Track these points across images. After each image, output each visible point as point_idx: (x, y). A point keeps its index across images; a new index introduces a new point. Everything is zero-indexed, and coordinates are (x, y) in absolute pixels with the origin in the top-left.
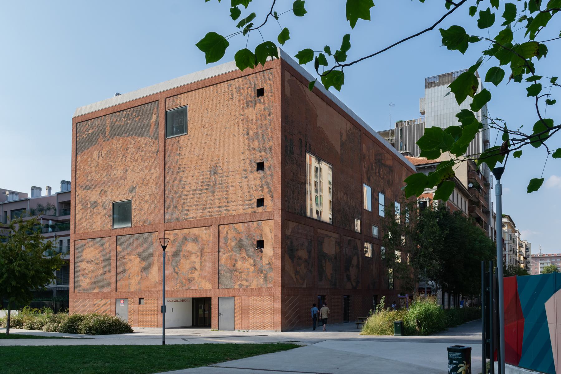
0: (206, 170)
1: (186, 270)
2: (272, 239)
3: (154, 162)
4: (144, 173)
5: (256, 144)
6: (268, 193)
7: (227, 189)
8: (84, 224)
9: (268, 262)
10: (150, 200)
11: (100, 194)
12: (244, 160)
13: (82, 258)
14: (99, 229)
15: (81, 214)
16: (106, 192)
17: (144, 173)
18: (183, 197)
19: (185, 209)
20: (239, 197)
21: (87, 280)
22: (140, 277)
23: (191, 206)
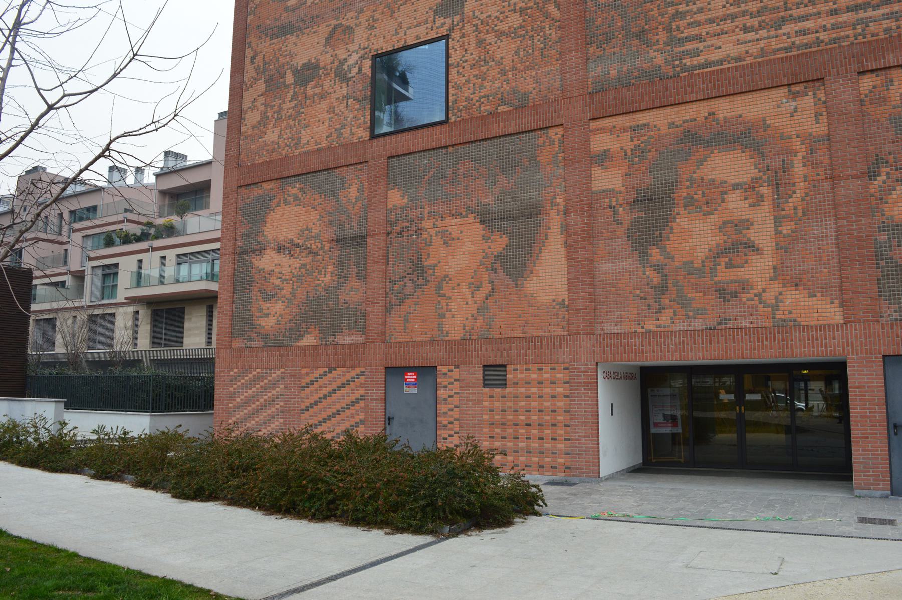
1: (701, 253)
8: (271, 136)
10: (521, 26)
11: (327, 39)
13: (260, 239)
14: (324, 144)
15: (262, 108)
16: (349, 30)
21: (278, 307)
22: (486, 288)
23: (711, 21)
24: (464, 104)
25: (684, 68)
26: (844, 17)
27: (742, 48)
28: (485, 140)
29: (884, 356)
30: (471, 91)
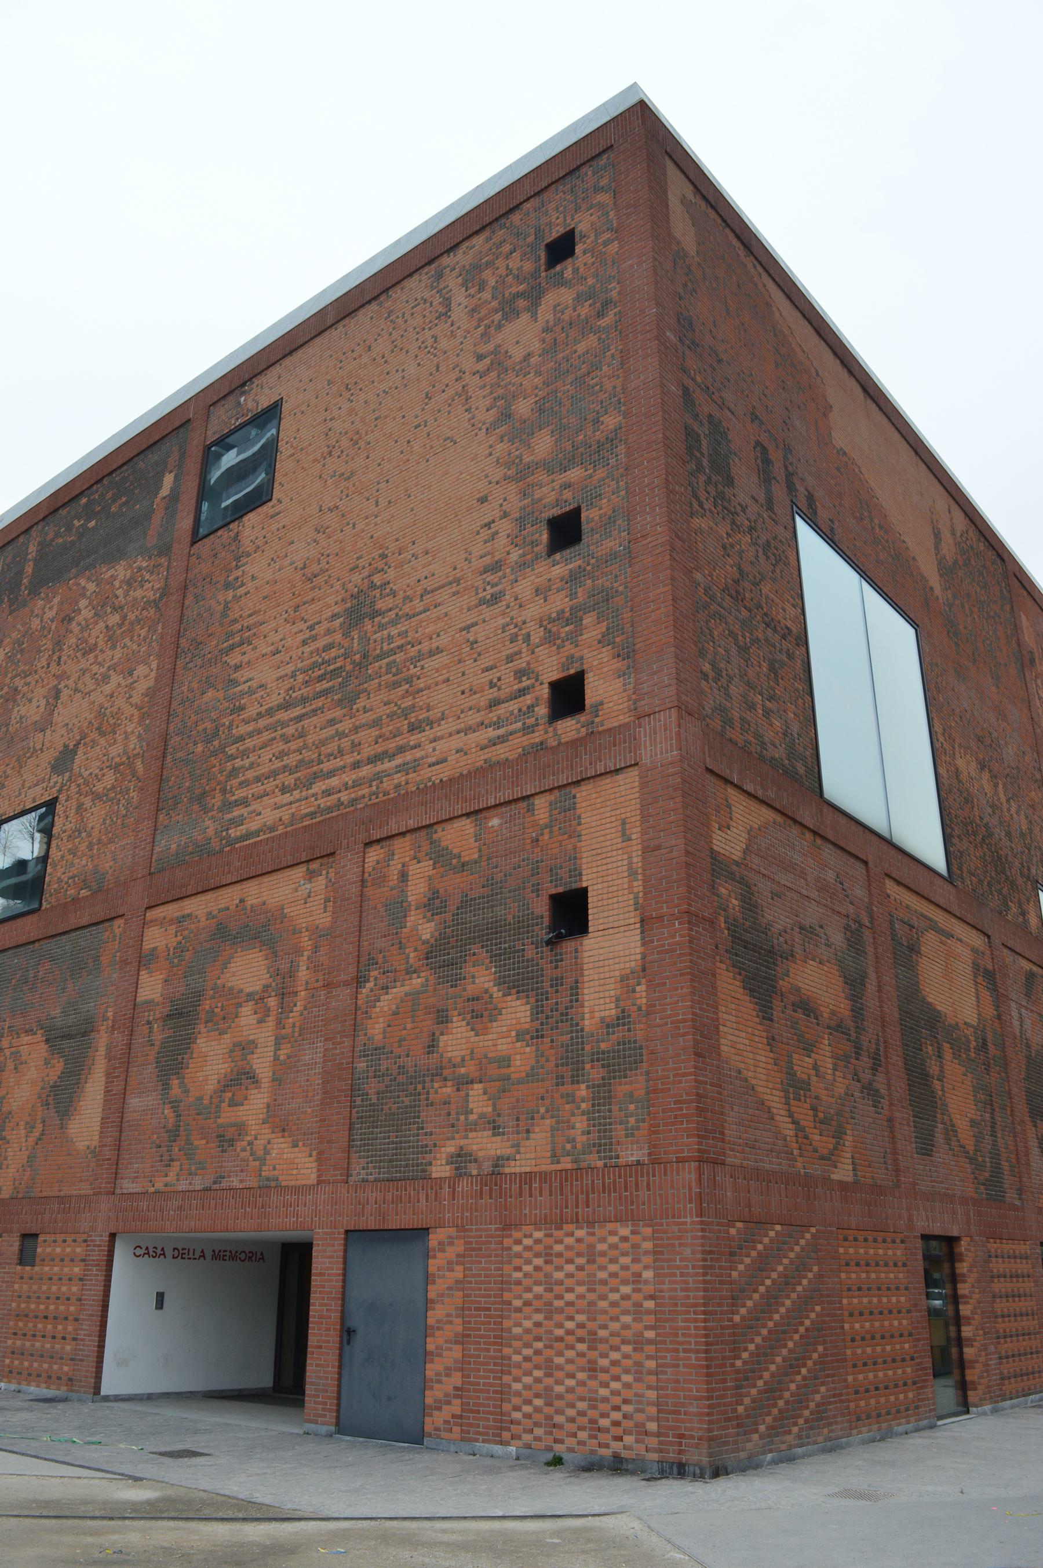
0: (330, 614)
1: (211, 1086)
2: (632, 873)
3: (145, 640)
4: (108, 689)
5: (543, 444)
6: (604, 641)
7: (413, 671)
9: (611, 1011)
10: (113, 788)
12: (488, 525)
17: (108, 689)
18: (231, 750)
19: (235, 798)
20: (463, 693)
22: (36, 1133)
23: (258, 779)
24: (56, 886)
25: (231, 842)
26: (366, 771)
27: (277, 814)
28: (64, 933)
29: (347, 1232)
30: (62, 870)
